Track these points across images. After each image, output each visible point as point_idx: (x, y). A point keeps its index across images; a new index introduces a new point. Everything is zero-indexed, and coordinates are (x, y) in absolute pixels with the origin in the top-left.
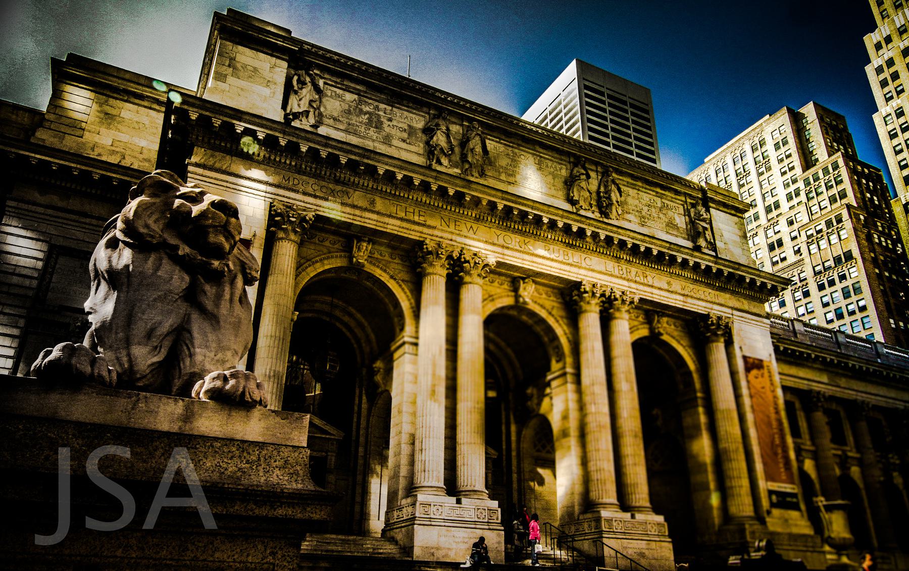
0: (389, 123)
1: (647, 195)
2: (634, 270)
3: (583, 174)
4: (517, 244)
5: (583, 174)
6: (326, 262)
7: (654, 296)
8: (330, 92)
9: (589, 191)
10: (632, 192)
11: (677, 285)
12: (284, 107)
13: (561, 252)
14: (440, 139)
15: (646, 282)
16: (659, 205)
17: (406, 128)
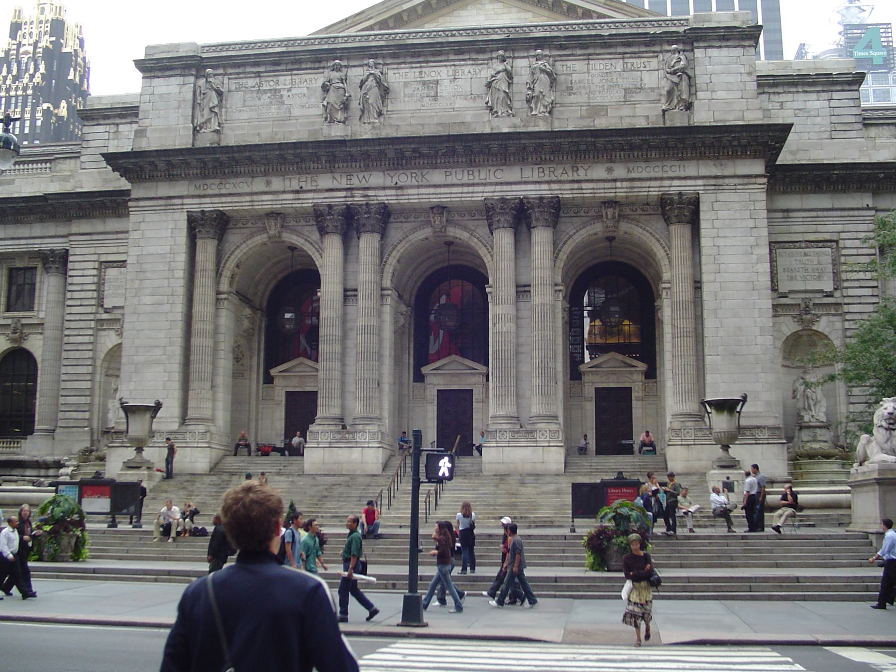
0: (290, 93)
1: (601, 62)
2: (559, 171)
3: (499, 72)
4: (413, 179)
5: (499, 72)
6: (249, 242)
7: (584, 191)
8: (234, 85)
9: (504, 91)
10: (579, 65)
11: (620, 171)
12: (193, 122)
13: (466, 173)
14: (332, 97)
15: (576, 178)
16: (619, 67)
17: (305, 90)
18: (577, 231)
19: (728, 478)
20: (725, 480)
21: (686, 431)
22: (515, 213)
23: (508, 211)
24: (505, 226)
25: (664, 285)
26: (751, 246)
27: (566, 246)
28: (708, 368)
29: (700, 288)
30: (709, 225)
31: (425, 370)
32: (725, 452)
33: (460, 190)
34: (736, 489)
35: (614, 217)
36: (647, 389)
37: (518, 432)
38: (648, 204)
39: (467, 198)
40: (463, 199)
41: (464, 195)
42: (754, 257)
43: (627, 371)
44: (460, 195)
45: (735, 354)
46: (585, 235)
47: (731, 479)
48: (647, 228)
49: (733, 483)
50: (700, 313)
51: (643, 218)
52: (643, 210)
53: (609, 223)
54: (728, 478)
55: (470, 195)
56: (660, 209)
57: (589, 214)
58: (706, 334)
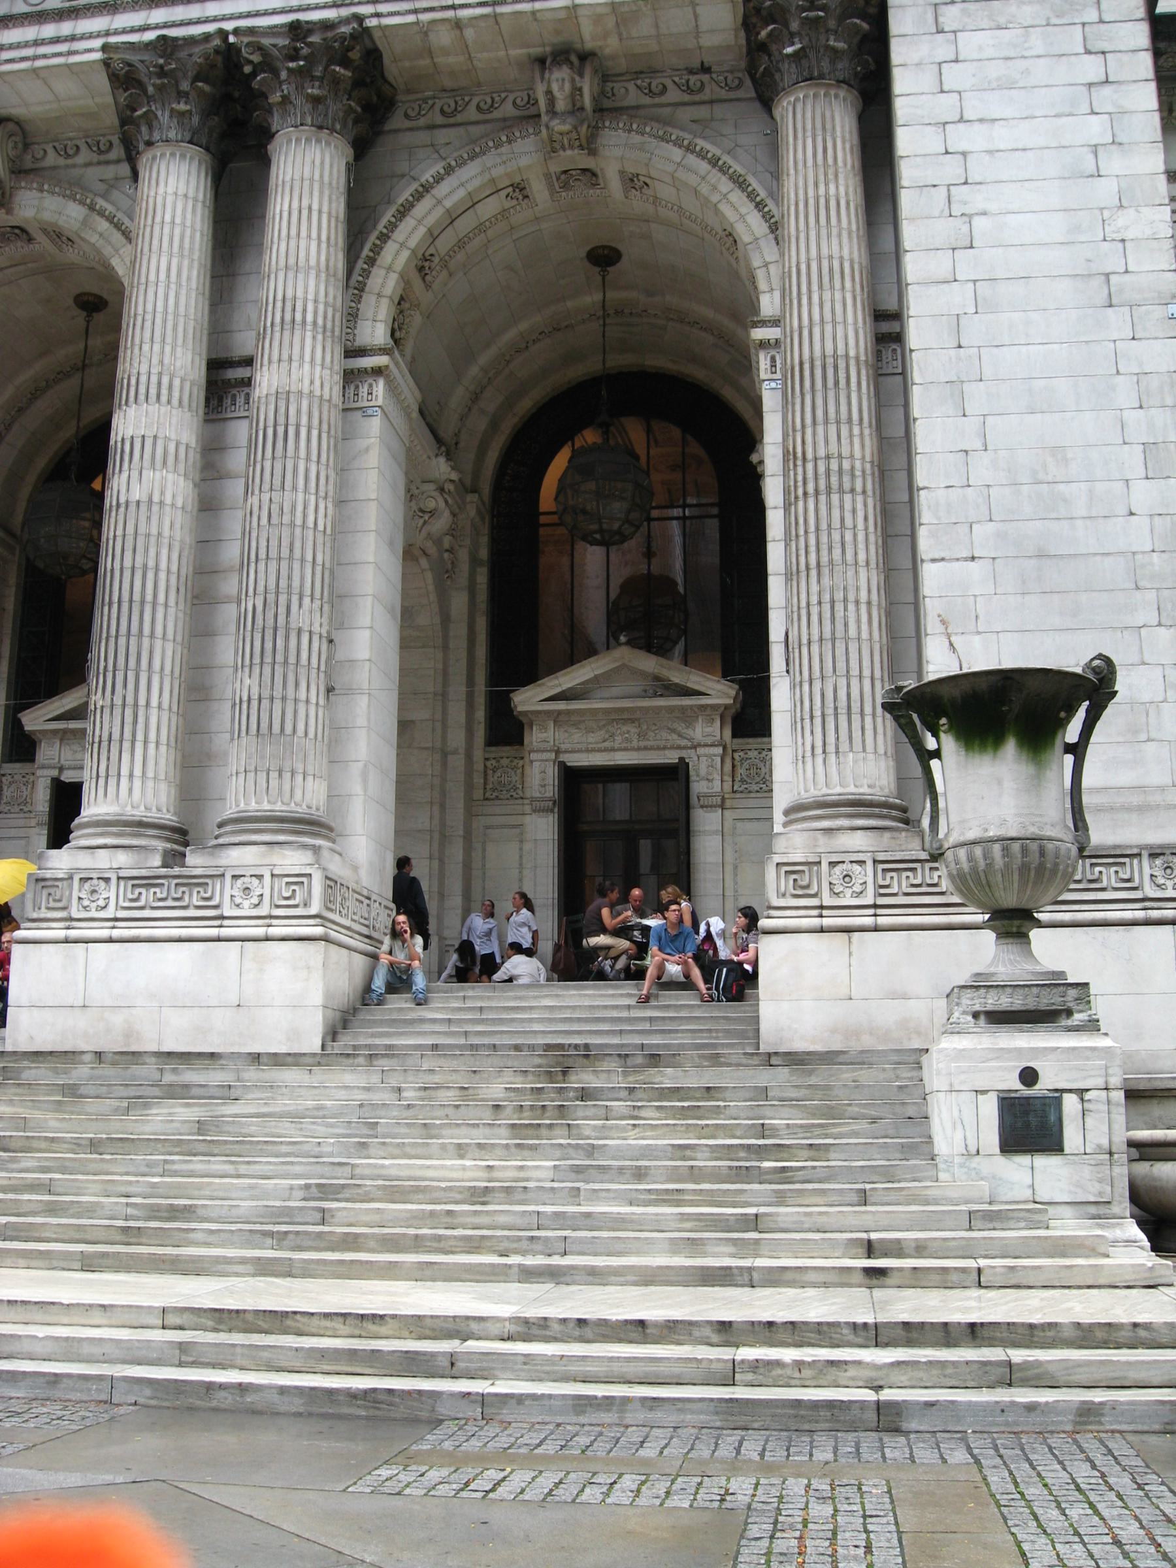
18: (449, 170)
19: (1029, 1076)
20: (1013, 1083)
21: (838, 870)
22: (207, 88)
23: (185, 86)
24: (172, 135)
25: (758, 334)
26: (1095, 149)
27: (408, 223)
28: (932, 608)
29: (898, 338)
30: (927, 80)
31: (34, 720)
32: (1011, 951)
33: (29, 33)
34: (1072, 1137)
35: (576, 109)
36: (741, 771)
37: (148, 882)
38: (705, 69)
39: (53, 57)
40: (40, 63)
41: (42, 50)
42: (1105, 190)
43: (671, 709)
44: (28, 52)
45: (1041, 555)
46: (477, 183)
47: (1047, 1082)
48: (701, 143)
49: (1058, 1102)
50: (902, 433)
51: (685, 114)
52: (689, 90)
53: (558, 126)
54: (1029, 1076)
55: (63, 48)
56: (748, 82)
57: (496, 114)
58: (921, 479)
